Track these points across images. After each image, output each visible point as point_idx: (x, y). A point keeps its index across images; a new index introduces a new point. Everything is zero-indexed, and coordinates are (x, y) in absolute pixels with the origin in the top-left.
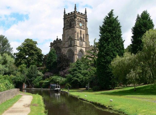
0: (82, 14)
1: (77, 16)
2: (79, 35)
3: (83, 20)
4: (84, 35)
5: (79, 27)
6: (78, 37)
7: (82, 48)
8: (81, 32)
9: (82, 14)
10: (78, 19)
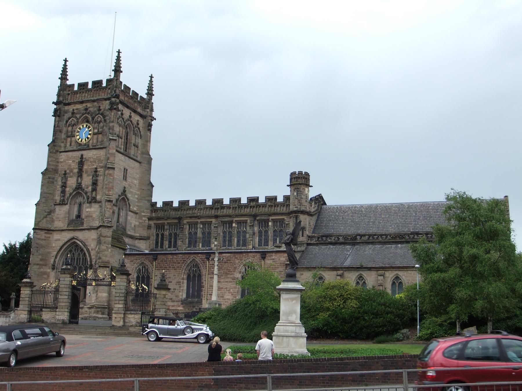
0: (100, 82)
1: (69, 104)
2: (72, 182)
3: (100, 110)
4: (96, 171)
5: (75, 148)
6: (63, 192)
7: (80, 235)
8: (81, 163)
9: (97, 84)
10: (73, 113)
